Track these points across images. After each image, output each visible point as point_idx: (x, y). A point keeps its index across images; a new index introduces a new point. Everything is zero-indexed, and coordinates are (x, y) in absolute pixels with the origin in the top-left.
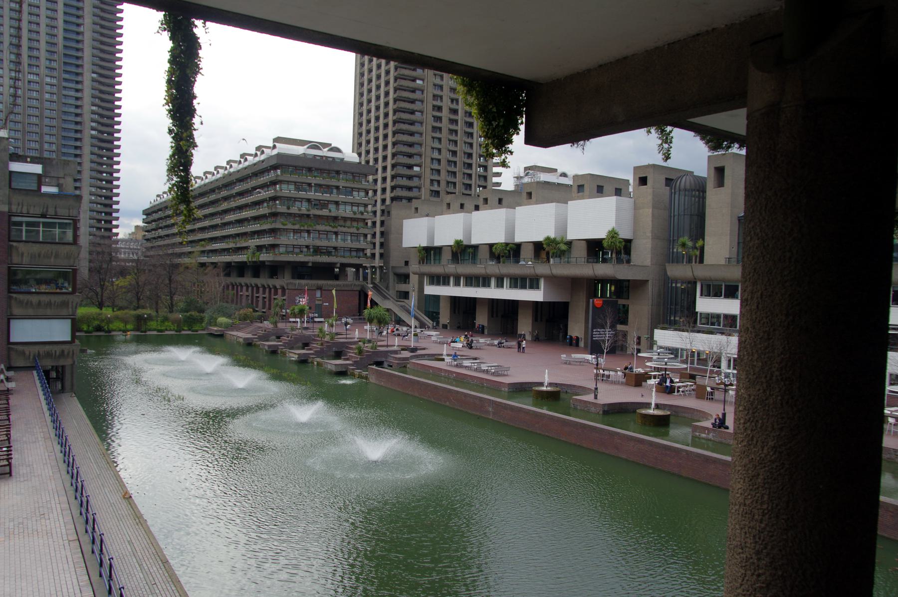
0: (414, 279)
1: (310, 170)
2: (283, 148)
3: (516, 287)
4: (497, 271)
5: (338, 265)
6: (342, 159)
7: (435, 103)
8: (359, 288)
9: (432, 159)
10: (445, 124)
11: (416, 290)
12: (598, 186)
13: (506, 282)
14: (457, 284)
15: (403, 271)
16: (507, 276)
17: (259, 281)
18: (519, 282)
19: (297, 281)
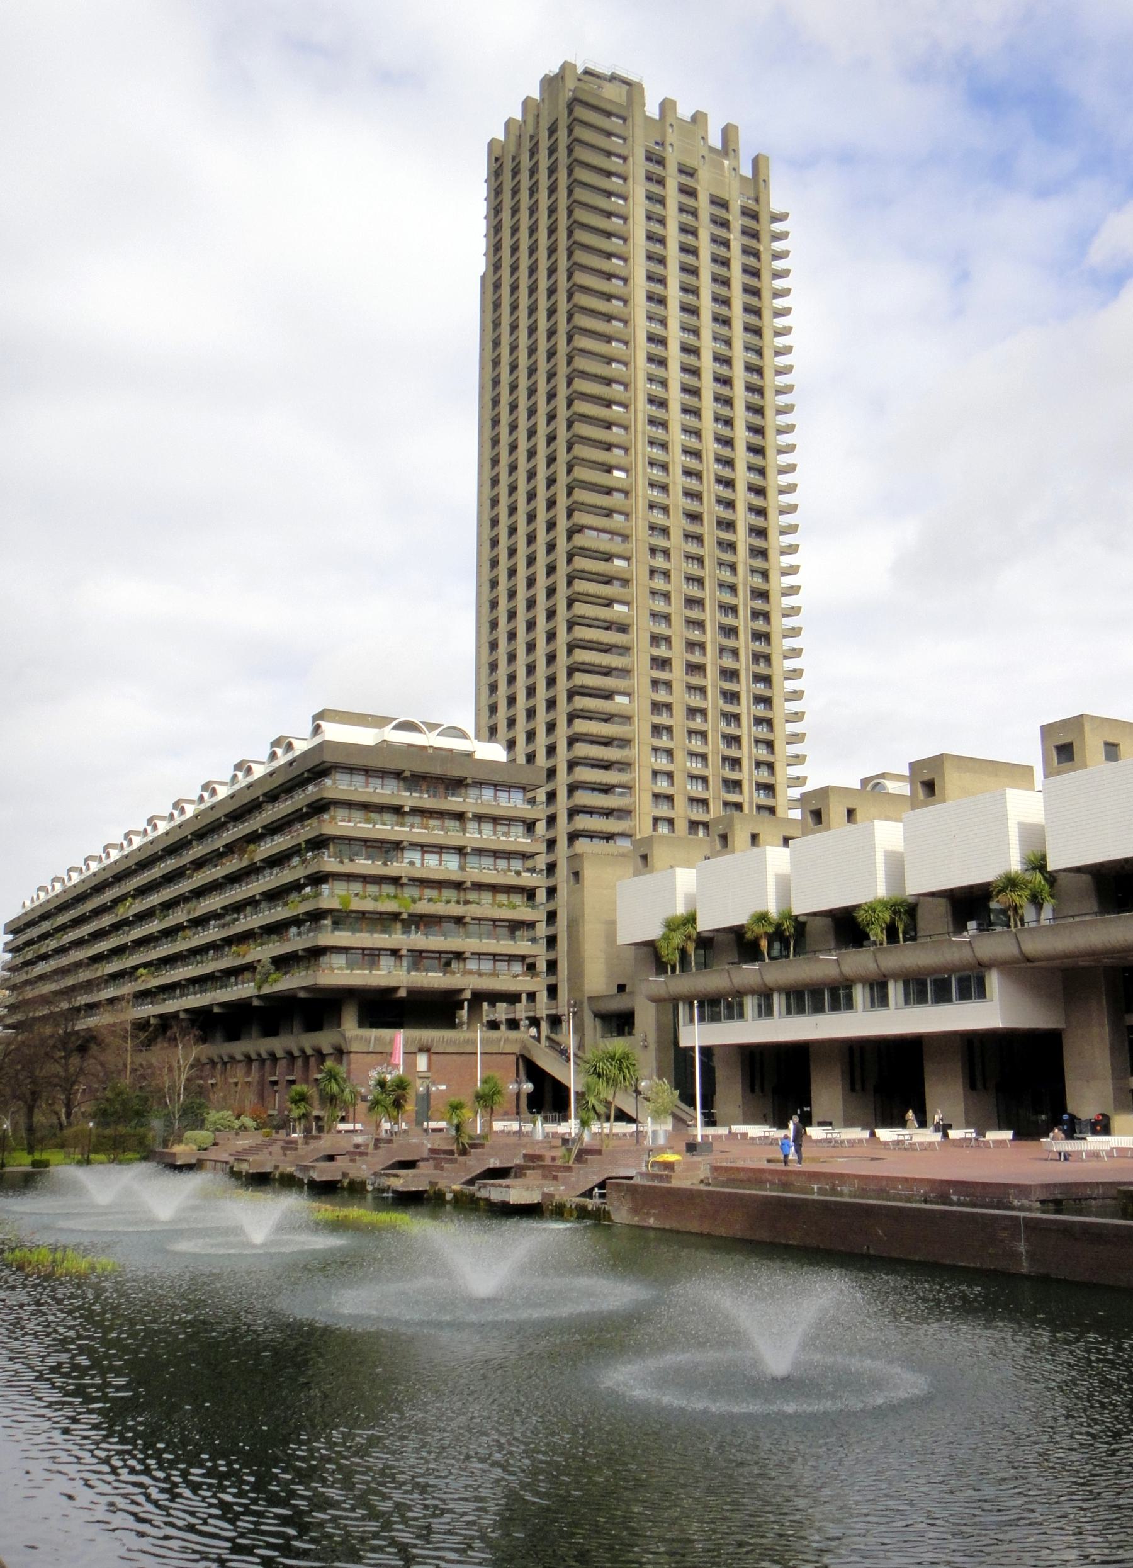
0: (646, 1019)
1: (398, 775)
2: (334, 732)
3: (921, 999)
4: (872, 966)
5: (467, 995)
6: (469, 755)
7: (656, 652)
8: (516, 1049)
9: (655, 773)
10: (680, 698)
11: (652, 1046)
12: (1107, 744)
13: (895, 991)
14: (766, 1010)
15: (618, 1004)
16: (896, 976)
17: (278, 1044)
18: (928, 987)
19: (374, 1033)
